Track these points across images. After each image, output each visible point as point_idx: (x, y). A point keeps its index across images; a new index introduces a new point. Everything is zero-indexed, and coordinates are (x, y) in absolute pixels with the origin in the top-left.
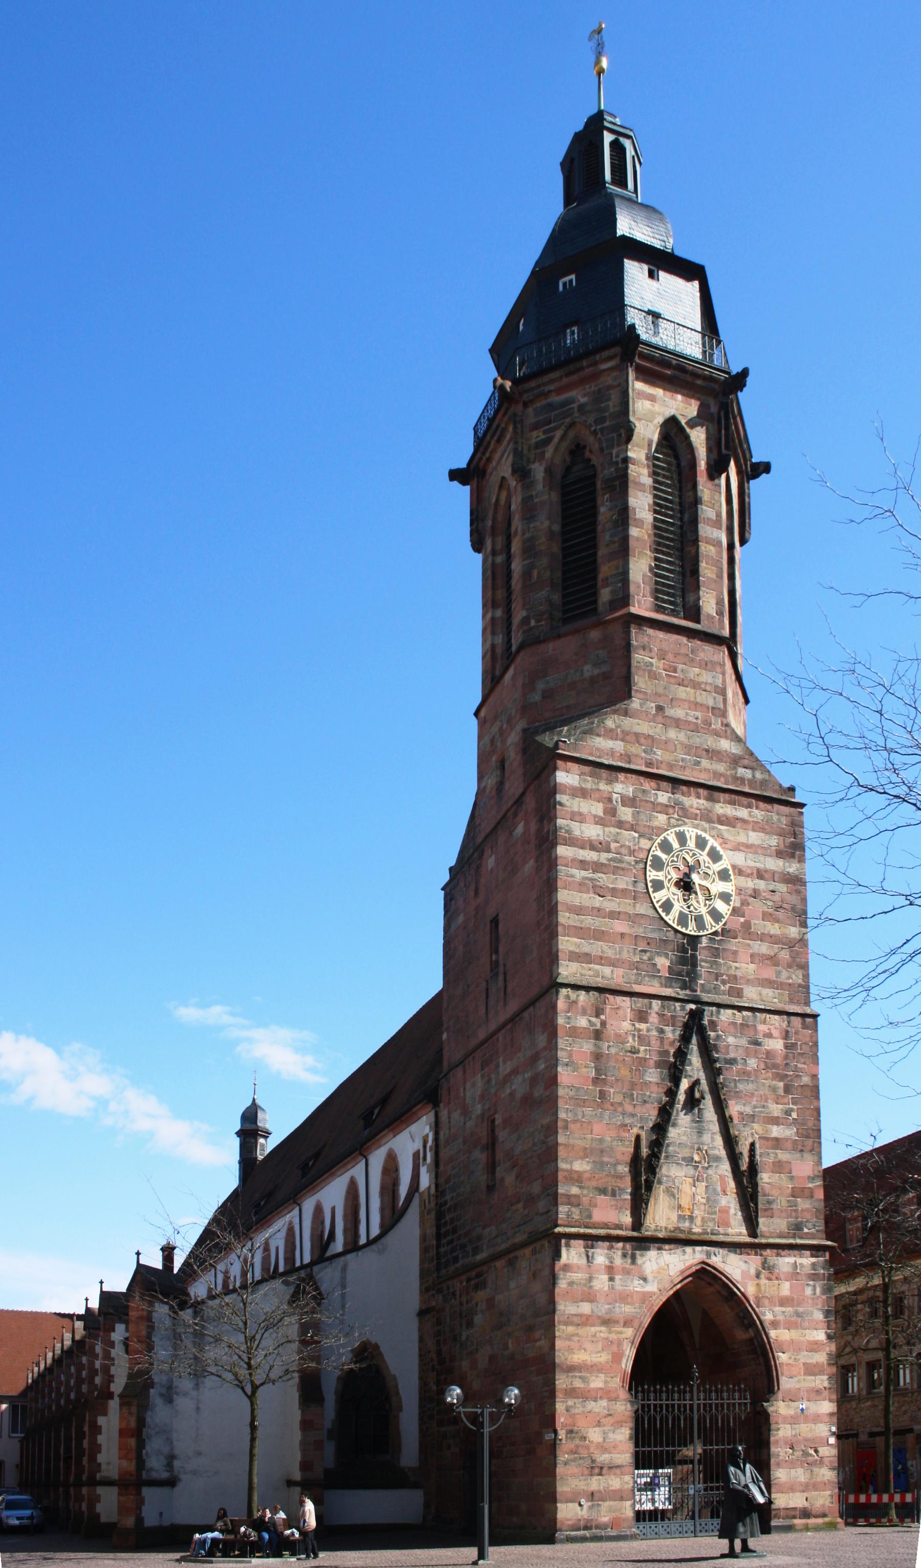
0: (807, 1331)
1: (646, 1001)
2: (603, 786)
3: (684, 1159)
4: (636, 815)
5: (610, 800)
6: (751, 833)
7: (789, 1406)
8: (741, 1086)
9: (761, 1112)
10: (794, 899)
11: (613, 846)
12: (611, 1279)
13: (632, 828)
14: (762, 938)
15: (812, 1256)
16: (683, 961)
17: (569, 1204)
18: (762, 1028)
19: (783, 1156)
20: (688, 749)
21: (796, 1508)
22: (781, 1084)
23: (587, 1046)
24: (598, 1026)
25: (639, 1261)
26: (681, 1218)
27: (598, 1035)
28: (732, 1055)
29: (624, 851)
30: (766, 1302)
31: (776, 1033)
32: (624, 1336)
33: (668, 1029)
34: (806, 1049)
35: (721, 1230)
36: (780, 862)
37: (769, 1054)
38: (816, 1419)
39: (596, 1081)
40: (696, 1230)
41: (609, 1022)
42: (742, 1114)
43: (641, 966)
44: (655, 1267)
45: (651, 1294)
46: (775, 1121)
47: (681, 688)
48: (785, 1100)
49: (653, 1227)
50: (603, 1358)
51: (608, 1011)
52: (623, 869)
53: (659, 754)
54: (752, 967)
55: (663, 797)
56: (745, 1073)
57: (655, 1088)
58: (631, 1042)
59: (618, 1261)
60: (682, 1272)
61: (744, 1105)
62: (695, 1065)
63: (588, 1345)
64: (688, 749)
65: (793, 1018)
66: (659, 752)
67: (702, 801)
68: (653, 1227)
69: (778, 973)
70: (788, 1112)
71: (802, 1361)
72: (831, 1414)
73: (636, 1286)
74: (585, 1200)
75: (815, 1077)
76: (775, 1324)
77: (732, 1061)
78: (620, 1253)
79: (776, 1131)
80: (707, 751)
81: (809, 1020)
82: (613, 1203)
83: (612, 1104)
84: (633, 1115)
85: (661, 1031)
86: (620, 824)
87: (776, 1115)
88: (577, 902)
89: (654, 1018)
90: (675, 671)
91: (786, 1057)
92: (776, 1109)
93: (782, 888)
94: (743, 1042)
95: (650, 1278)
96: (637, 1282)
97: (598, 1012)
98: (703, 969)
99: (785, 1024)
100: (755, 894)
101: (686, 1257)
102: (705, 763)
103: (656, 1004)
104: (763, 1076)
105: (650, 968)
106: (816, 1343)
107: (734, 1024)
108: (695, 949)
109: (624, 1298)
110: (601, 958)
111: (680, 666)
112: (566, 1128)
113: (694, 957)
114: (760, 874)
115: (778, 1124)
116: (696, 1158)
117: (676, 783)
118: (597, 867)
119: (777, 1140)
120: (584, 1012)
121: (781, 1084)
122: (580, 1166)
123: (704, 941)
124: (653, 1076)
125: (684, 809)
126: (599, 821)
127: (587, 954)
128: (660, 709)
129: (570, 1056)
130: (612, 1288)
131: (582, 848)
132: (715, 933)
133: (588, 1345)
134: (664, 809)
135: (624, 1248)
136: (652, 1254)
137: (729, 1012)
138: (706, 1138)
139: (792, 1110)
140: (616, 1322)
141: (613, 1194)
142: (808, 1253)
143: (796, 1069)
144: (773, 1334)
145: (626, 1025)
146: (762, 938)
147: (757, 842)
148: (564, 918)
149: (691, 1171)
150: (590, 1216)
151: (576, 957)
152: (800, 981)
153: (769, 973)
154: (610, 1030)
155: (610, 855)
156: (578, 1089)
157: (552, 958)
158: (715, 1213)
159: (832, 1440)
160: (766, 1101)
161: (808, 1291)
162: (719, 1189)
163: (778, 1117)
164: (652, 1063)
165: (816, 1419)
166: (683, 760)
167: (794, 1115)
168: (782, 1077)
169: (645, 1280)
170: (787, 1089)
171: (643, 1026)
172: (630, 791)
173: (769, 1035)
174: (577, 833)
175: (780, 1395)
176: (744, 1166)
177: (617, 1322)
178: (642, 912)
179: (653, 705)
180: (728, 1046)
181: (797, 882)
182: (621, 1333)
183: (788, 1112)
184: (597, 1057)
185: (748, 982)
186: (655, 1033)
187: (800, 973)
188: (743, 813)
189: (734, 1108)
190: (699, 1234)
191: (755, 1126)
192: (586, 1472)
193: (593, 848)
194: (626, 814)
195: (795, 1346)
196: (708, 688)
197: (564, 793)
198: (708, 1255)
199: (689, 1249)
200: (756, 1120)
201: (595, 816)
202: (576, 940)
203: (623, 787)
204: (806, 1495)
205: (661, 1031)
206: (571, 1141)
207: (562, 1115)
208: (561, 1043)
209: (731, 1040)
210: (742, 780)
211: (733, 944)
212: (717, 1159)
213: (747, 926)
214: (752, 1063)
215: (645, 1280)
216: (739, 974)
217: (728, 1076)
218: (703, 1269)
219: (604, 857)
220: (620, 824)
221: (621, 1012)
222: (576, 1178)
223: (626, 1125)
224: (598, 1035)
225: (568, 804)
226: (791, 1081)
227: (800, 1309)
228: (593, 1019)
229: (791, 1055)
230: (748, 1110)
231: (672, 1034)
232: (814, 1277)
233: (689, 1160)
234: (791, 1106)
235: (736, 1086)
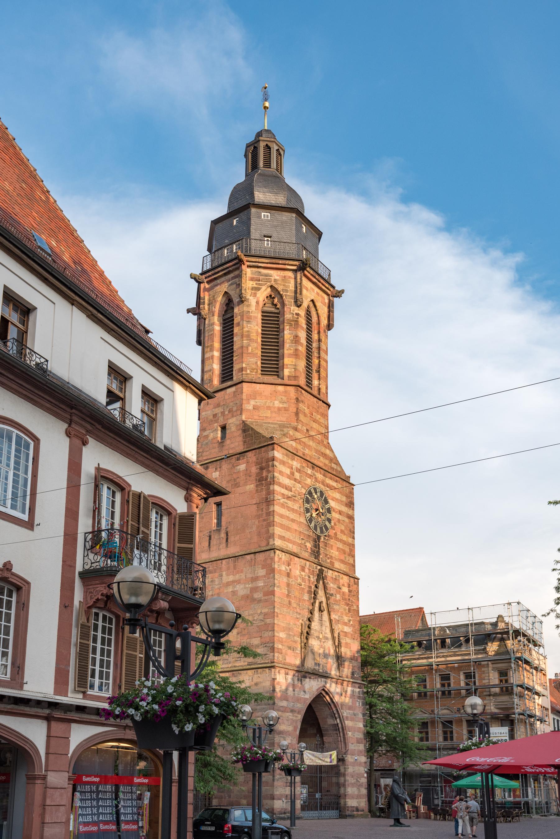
0: (357, 723)
1: (304, 561)
2: (290, 462)
3: (317, 637)
4: (301, 477)
5: (292, 468)
6: (337, 494)
7: (352, 758)
10: (350, 526)
11: (293, 489)
12: (294, 691)
13: (299, 483)
14: (341, 541)
15: (359, 688)
16: (315, 546)
17: (278, 652)
18: (341, 581)
20: (317, 451)
21: (354, 807)
22: (347, 608)
23: (285, 580)
24: (289, 571)
25: (303, 683)
26: (316, 664)
27: (288, 575)
28: (332, 592)
29: (297, 493)
30: (344, 707)
31: (346, 585)
32: (298, 718)
33: (311, 576)
34: (355, 593)
36: (346, 509)
37: (343, 593)
38: (360, 764)
39: (288, 596)
40: (321, 671)
41: (292, 570)
43: (302, 546)
44: (308, 687)
45: (307, 699)
46: (345, 624)
47: (314, 423)
49: (306, 667)
50: (290, 728)
51: (292, 564)
52: (296, 501)
53: (307, 451)
54: (337, 553)
55: (309, 471)
56: (336, 601)
57: (307, 603)
58: (299, 581)
59: (296, 682)
60: (317, 690)
62: (321, 593)
63: (285, 722)
64: (317, 451)
65: (351, 578)
66: (307, 450)
67: (322, 476)
68: (306, 667)
69: (345, 558)
70: (349, 621)
71: (356, 736)
72: (365, 763)
73: (302, 695)
74: (284, 651)
75: (358, 606)
76: (347, 718)
77: (332, 595)
78: (297, 678)
79: (347, 629)
80: (322, 453)
81: (356, 580)
82: (293, 654)
83: (293, 608)
84: (300, 614)
85: (309, 577)
86: (295, 480)
88: (281, 512)
89: (307, 570)
90: (312, 415)
91: (349, 596)
93: (347, 520)
94: (335, 587)
95: (307, 692)
96: (302, 693)
97: (289, 565)
98: (322, 550)
99: (348, 581)
100: (339, 520)
101: (319, 683)
102: (322, 459)
103: (308, 563)
105: (304, 547)
106: (360, 728)
107: (332, 578)
108: (319, 542)
109: (298, 700)
110: (289, 539)
111: (314, 414)
112: (277, 616)
113: (319, 544)
114: (340, 513)
115: (346, 626)
116: (321, 637)
117: (314, 466)
118: (288, 498)
119: (346, 632)
120: (284, 564)
122: (282, 635)
123: (322, 538)
124: (306, 597)
125: (316, 478)
126: (289, 477)
127: (284, 537)
128: (307, 430)
129: (279, 583)
130: (294, 694)
131: (283, 488)
132: (325, 536)
133: (285, 722)
134: (310, 476)
135: (298, 676)
136: (307, 680)
137: (331, 571)
138: (324, 628)
140: (295, 711)
141: (293, 650)
142: (357, 685)
143: (352, 602)
144: (346, 722)
145: (298, 572)
146: (341, 541)
147: (339, 498)
148: (277, 519)
149: (319, 643)
150: (285, 660)
151: (282, 538)
152: (352, 562)
153: (342, 557)
154: (293, 573)
155: (292, 493)
156: (282, 599)
157: (272, 536)
159: (365, 775)
161: (357, 704)
164: (306, 591)
165: (360, 764)
166: (315, 455)
167: (351, 623)
168: (348, 605)
169: (305, 692)
171: (303, 574)
172: (299, 466)
173: (343, 585)
174: (281, 481)
175: (349, 752)
176: (337, 644)
177: (295, 711)
178: (302, 521)
179: (305, 428)
180: (330, 588)
181: (351, 518)
182: (297, 717)
183: (349, 621)
184: (288, 585)
185: (336, 559)
186: (307, 577)
187: (352, 559)
188: (334, 484)
189: (333, 616)
191: (339, 625)
192: (285, 785)
193: (286, 489)
194: (297, 475)
195: (354, 729)
196: (323, 425)
197: (277, 461)
199: (319, 680)
201: (287, 474)
202: (280, 529)
203: (296, 464)
204: (357, 800)
205: (309, 577)
206: (279, 623)
207: (276, 610)
208: (276, 576)
209: (332, 585)
210: (333, 468)
211: (332, 542)
212: (327, 638)
213: (336, 534)
214: (338, 597)
215: (305, 692)
216: (333, 556)
217: (331, 601)
219: (290, 494)
220: (295, 480)
221: (296, 565)
222: (281, 641)
223: (297, 618)
224: (288, 575)
225: (278, 466)
227: (355, 712)
228: (287, 567)
230: (337, 618)
231: (313, 579)
232: (359, 697)
233: (318, 638)
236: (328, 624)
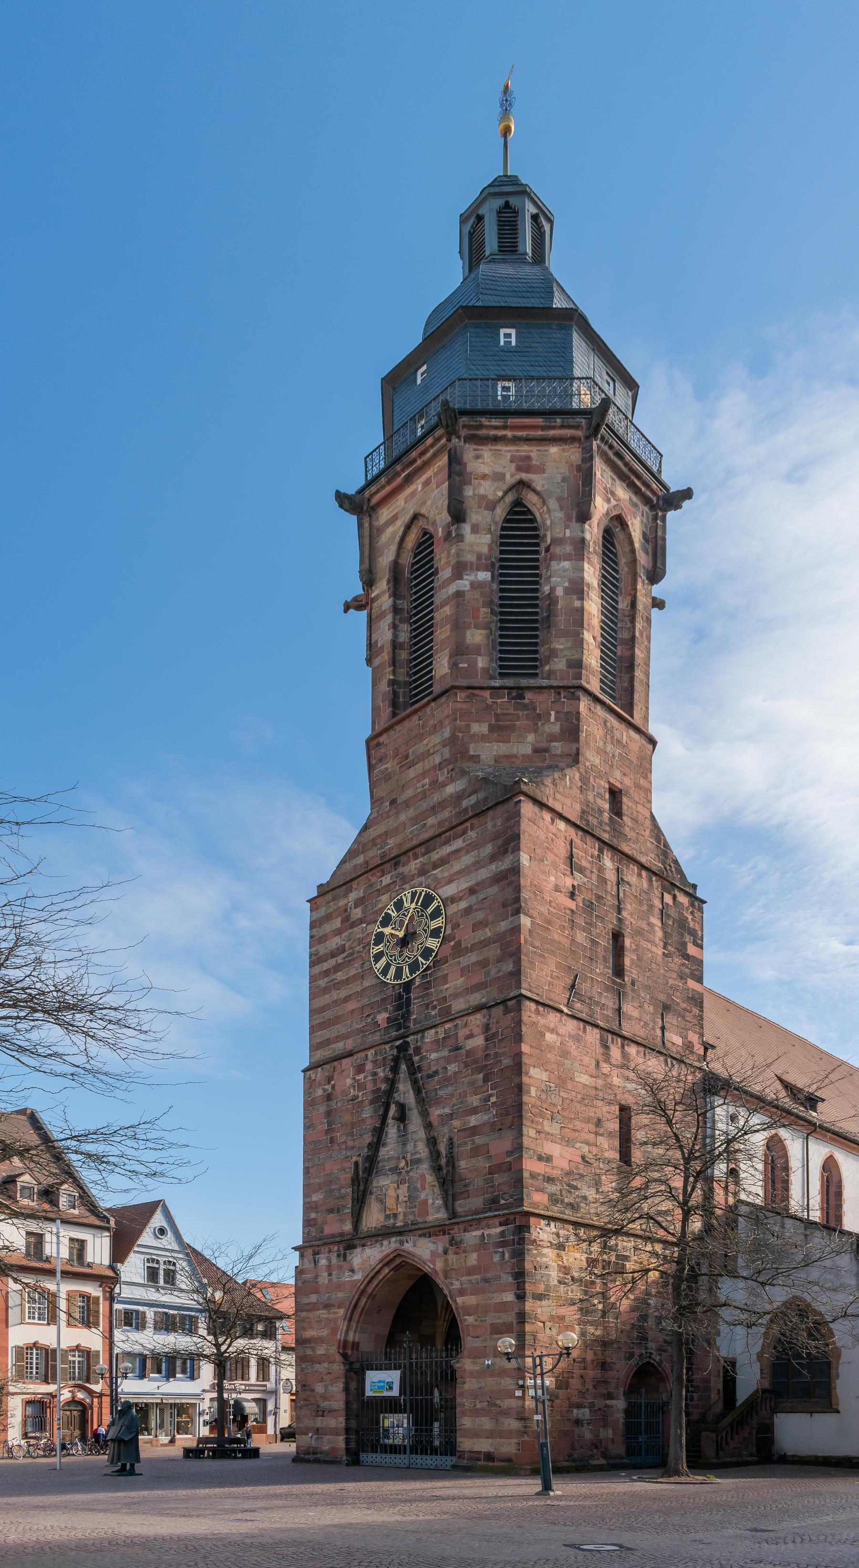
8: (440, 1093)
9: (460, 1108)
19: (479, 1140)
22: (481, 1076)
31: (476, 1031)
35: (420, 1220)
37: (469, 1053)
42: (441, 1115)
46: (474, 1111)
48: (484, 1089)
60: (381, 1261)
61: (444, 1107)
79: (473, 1121)
87: (475, 1104)
92: (474, 1100)
104: (463, 1075)
119: (475, 1127)
121: (481, 1076)
139: (491, 1095)
158: (415, 1207)
160: (465, 1096)
162: (419, 1186)
163: (477, 1107)
167: (493, 1099)
168: (479, 1070)
170: (486, 1079)
173: (470, 1036)
183: (487, 1099)
190: (401, 1227)
198: (402, 1243)
199: (385, 1242)
200: (454, 1116)
218: (399, 1255)
226: (491, 1069)
229: (491, 1045)
234: (490, 1092)
235: (436, 1094)
236: (422, 1134)
